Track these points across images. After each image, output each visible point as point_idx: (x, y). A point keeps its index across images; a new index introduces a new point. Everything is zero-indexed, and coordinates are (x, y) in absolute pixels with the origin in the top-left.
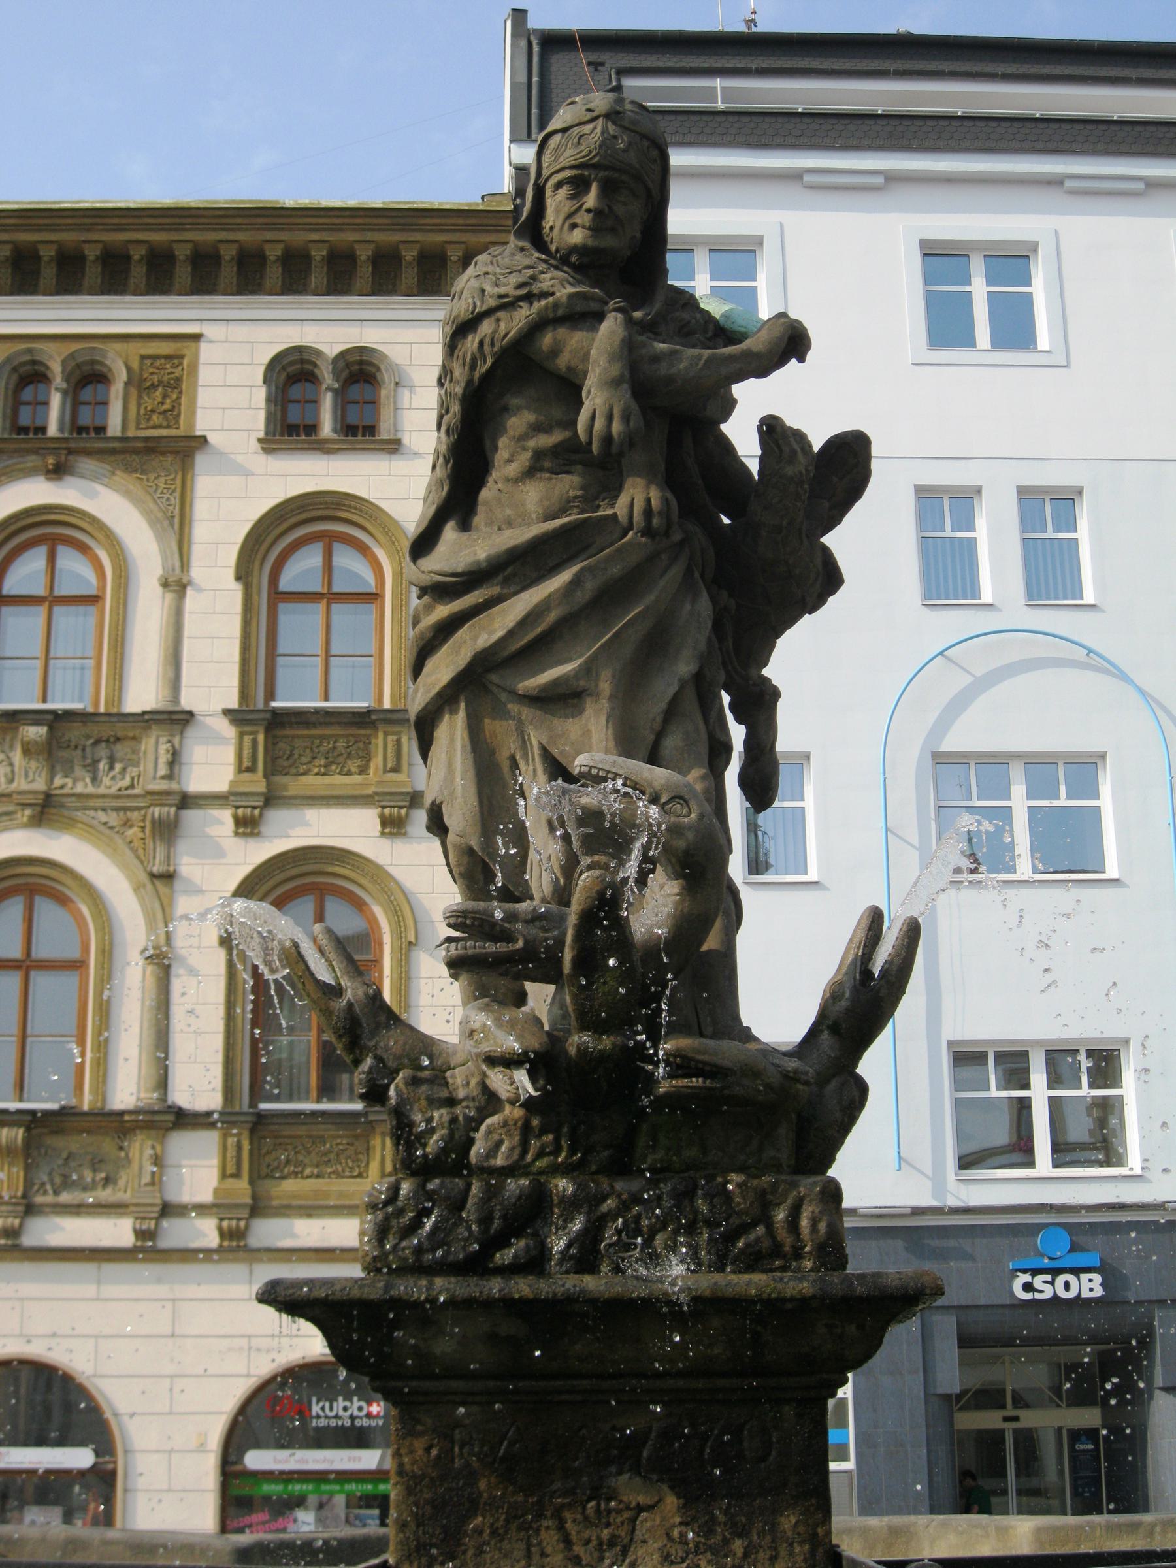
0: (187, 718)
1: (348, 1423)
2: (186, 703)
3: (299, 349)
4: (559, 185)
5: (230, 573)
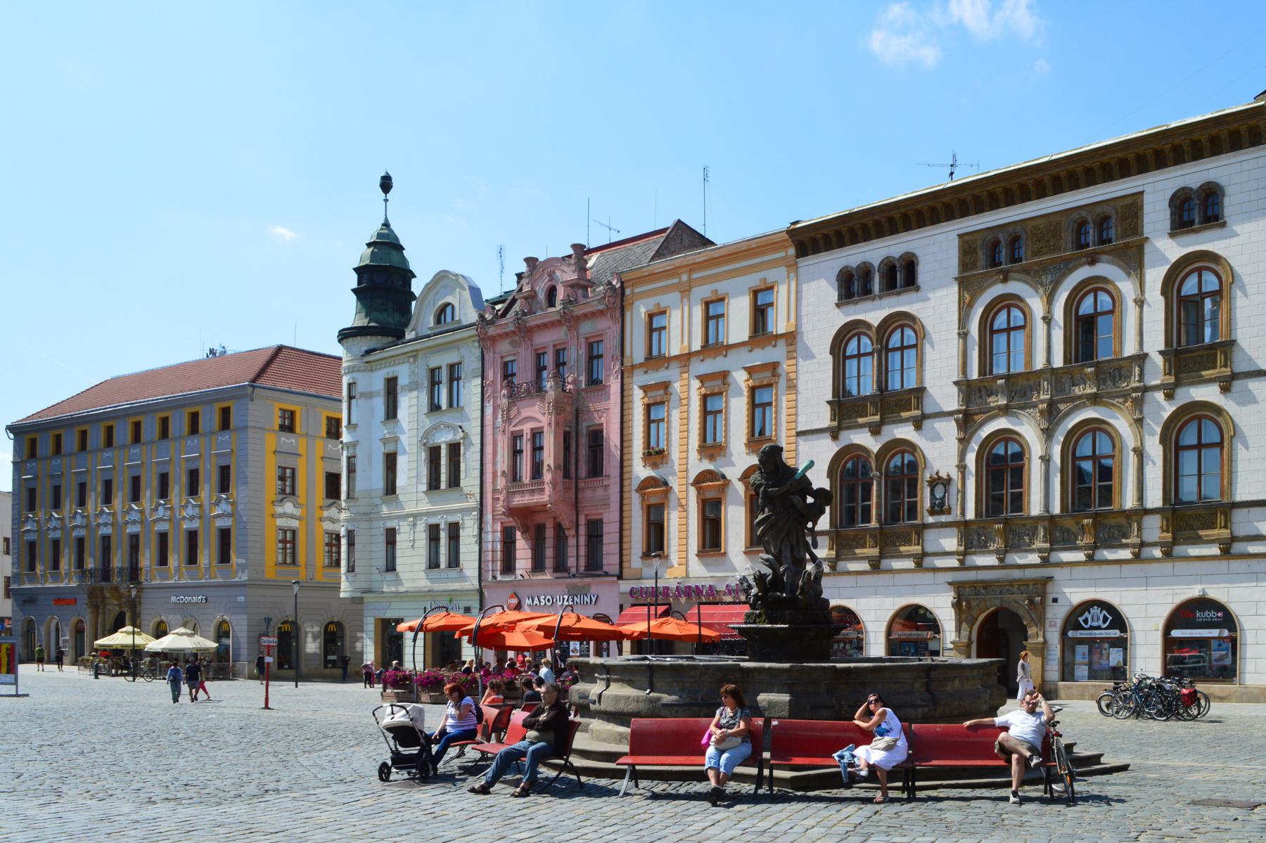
0: (1146, 355)
1: (1209, 620)
2: (1146, 350)
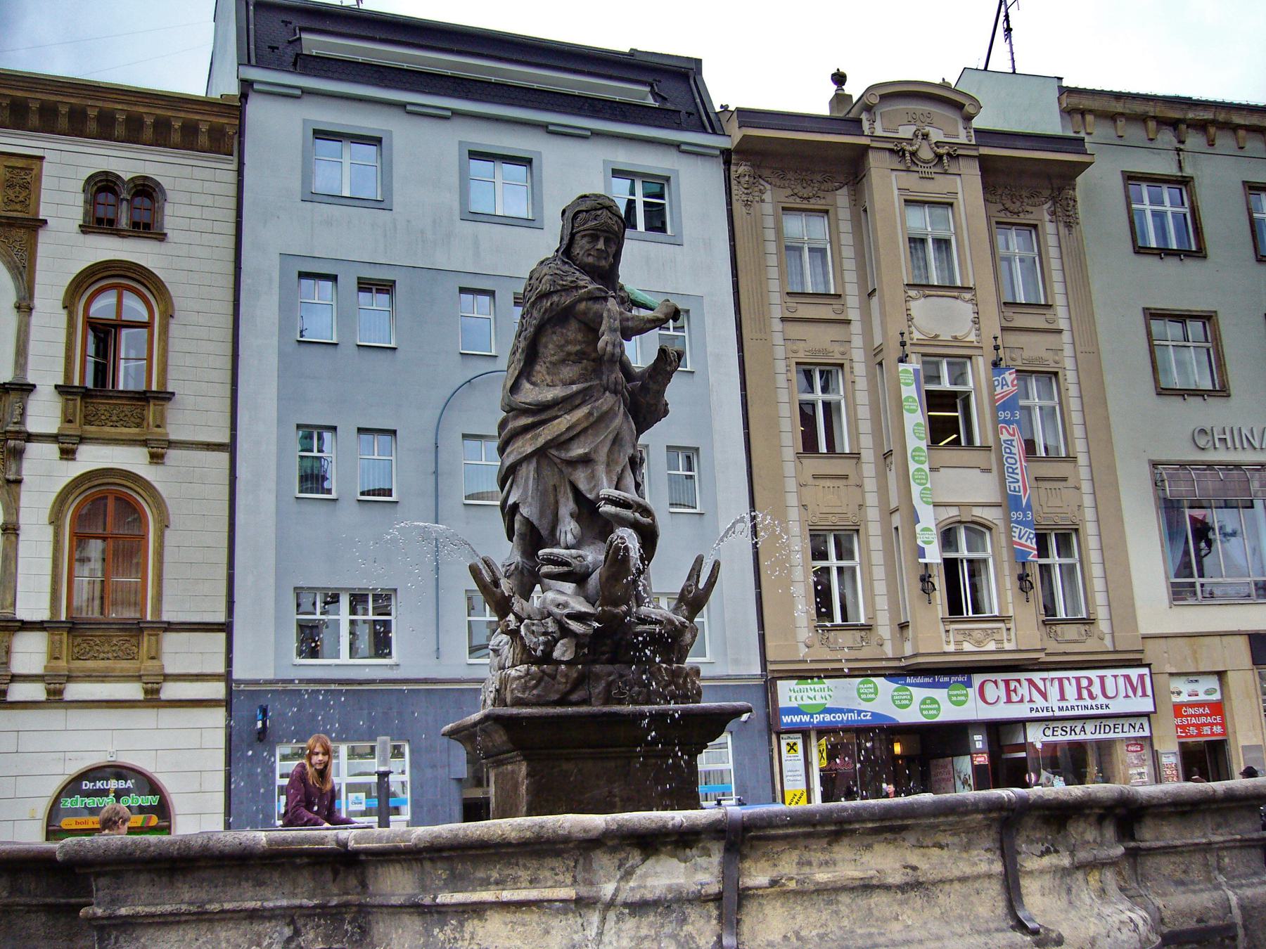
0: (29, 389)
3: (106, 173)
4: (583, 236)
5: (60, 304)
